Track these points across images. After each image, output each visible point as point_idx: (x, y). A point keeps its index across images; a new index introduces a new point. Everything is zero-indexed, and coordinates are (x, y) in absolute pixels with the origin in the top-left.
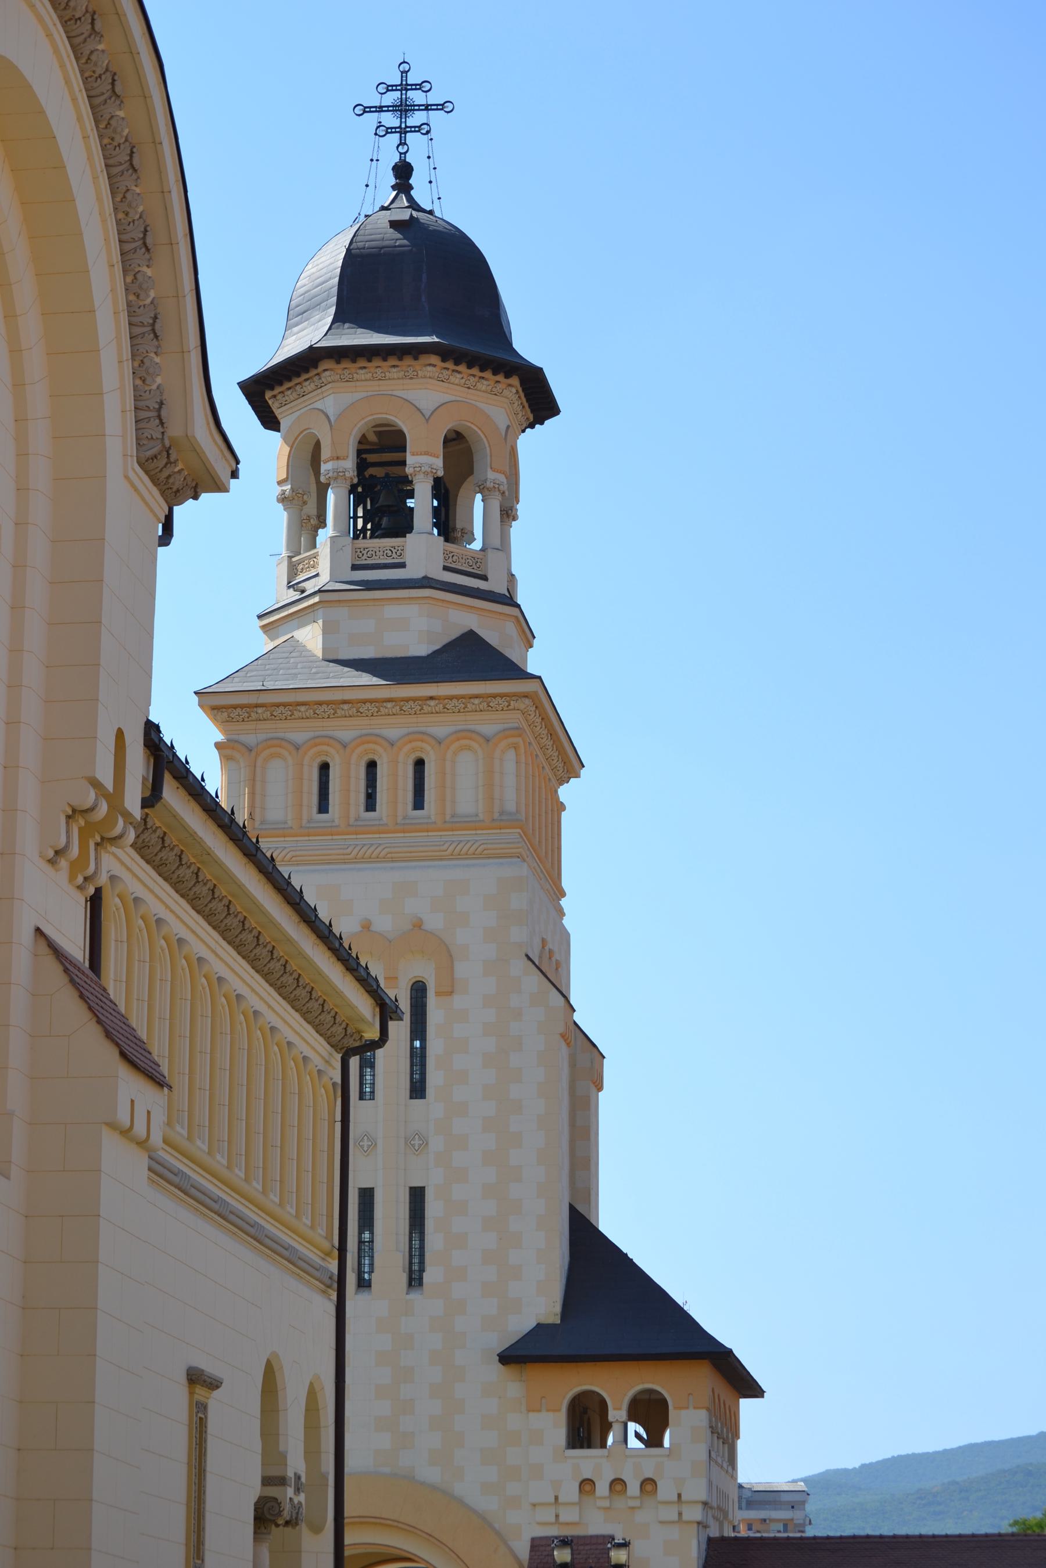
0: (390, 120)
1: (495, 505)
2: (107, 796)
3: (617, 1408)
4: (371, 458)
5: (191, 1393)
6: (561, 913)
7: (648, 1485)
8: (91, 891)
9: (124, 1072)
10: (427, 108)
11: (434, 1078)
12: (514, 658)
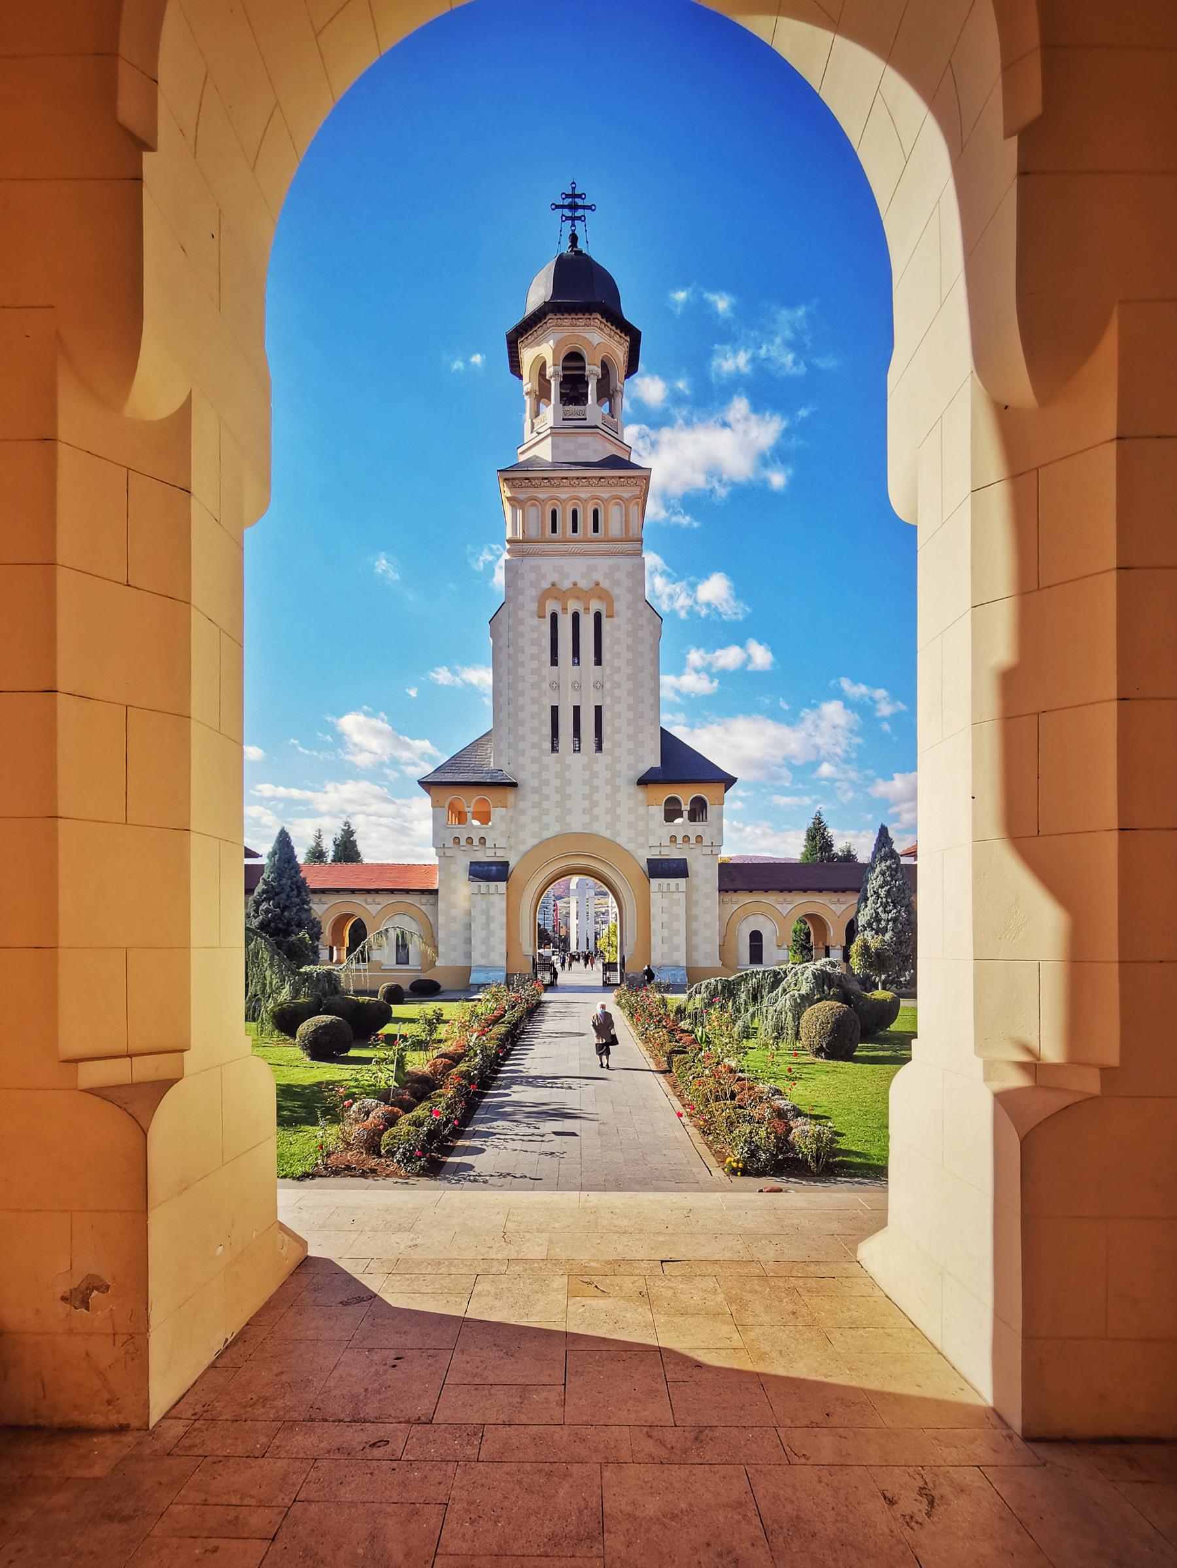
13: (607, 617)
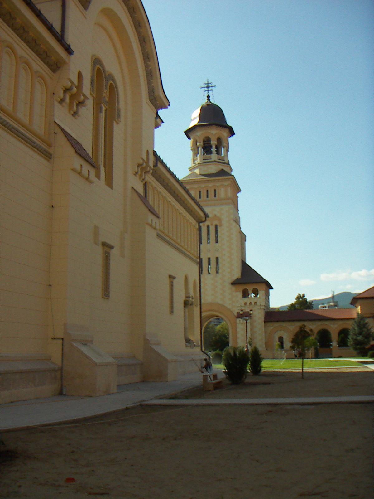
0: (206, 89)
1: (225, 149)
2: (145, 163)
3: (250, 291)
4: (205, 143)
5: (170, 279)
6: (238, 214)
7: (255, 303)
8: (144, 182)
9: (150, 214)
10: (212, 87)
11: (219, 240)
12: (229, 172)
13: (219, 226)
